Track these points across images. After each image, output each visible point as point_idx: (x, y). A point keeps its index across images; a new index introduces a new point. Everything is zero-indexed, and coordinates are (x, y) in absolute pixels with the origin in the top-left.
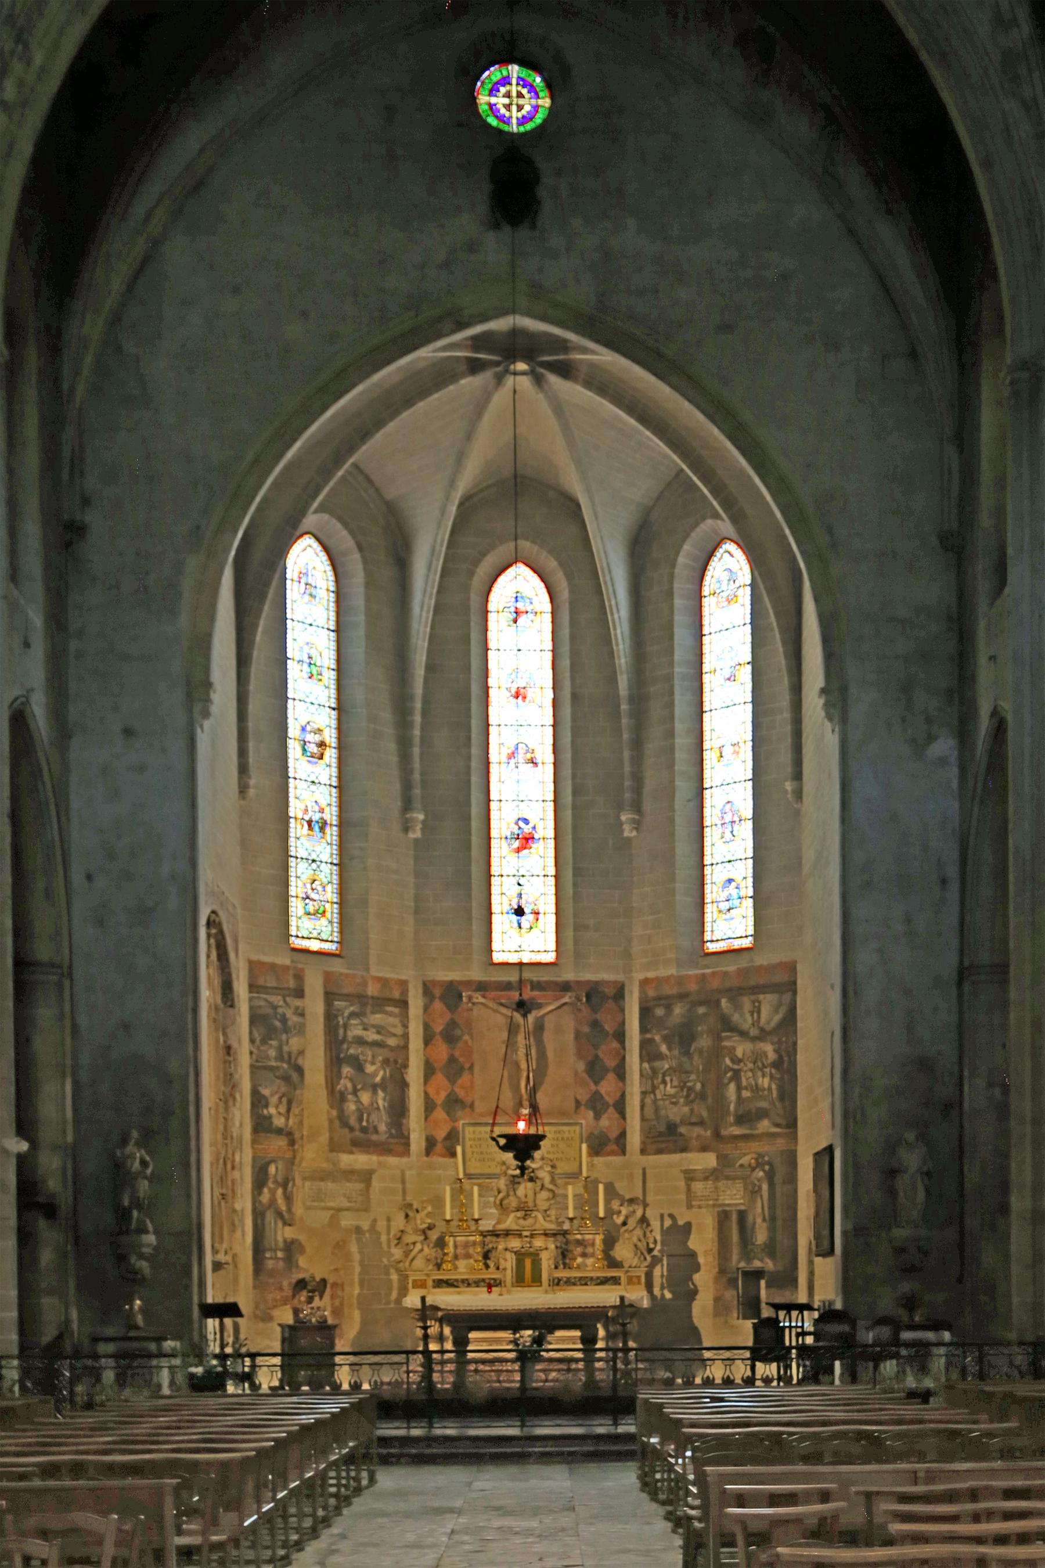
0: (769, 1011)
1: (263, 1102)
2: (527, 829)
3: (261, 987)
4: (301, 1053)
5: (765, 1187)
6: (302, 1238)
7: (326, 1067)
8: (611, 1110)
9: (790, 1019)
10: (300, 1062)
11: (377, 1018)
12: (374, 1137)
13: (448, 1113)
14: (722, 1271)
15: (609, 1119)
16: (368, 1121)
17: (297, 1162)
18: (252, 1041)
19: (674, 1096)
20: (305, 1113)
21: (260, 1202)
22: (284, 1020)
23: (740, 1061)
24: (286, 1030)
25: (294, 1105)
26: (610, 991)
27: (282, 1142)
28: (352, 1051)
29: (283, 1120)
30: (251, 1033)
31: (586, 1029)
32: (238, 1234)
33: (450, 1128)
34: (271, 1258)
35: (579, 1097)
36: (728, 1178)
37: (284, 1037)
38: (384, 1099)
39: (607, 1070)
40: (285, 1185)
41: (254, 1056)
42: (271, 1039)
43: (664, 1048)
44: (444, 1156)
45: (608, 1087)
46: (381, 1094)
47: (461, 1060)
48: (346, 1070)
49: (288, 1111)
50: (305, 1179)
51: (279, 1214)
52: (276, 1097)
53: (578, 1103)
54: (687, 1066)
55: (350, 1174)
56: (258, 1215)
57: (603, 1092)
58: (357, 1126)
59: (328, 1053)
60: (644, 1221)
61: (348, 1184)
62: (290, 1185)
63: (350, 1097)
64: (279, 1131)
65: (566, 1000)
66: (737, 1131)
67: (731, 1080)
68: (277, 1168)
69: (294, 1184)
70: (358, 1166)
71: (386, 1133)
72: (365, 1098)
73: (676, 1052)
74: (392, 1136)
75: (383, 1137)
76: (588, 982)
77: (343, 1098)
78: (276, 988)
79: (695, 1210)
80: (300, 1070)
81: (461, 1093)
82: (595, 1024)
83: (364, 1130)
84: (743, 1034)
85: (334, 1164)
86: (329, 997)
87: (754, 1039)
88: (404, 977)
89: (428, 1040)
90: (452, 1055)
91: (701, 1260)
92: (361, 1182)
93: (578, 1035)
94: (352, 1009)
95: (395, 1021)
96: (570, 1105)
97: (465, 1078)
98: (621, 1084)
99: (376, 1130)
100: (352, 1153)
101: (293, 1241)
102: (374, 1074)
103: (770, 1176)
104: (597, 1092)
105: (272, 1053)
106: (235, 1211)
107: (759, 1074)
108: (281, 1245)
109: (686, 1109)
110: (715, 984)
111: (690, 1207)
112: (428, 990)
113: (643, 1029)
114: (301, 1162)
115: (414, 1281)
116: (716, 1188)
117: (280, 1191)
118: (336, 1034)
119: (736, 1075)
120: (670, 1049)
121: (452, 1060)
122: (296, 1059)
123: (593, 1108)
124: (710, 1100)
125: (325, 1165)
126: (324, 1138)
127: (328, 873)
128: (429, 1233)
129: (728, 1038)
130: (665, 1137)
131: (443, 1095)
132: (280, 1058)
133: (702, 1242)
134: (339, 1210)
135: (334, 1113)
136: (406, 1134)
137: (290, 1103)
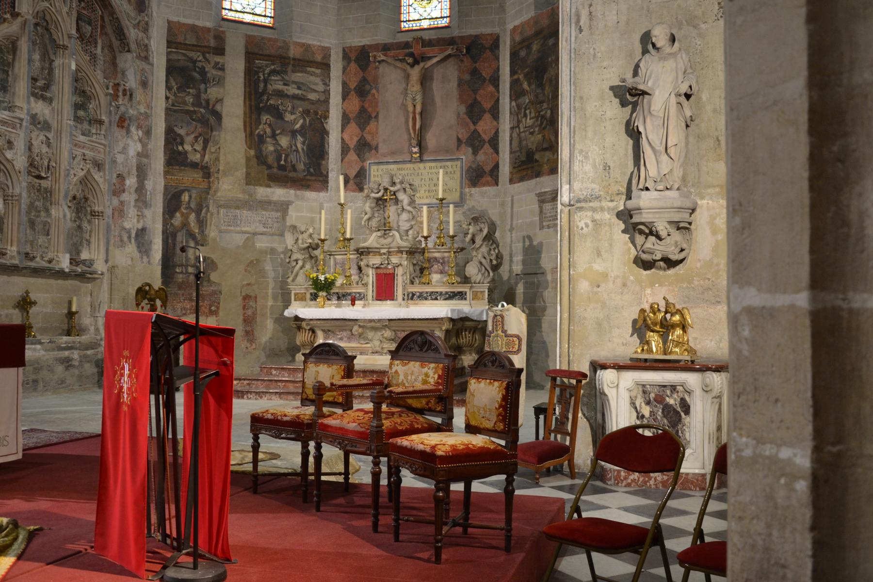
1: (179, 140)
3: (181, 43)
4: (220, 101)
7: (245, 113)
8: (487, 146)
10: (218, 108)
11: (298, 77)
12: (292, 174)
13: (358, 155)
15: (486, 154)
18: (168, 88)
19: (532, 127)
20: (222, 151)
21: (172, 224)
22: (203, 72)
24: (205, 80)
25: (211, 144)
27: (197, 175)
28: (272, 102)
29: (198, 156)
30: (167, 81)
31: (467, 77)
34: (182, 273)
35: (460, 137)
37: (202, 86)
38: (303, 143)
39: (485, 112)
40: (198, 212)
41: (170, 101)
42: (189, 88)
43: (525, 86)
44: (354, 191)
45: (485, 126)
46: (300, 139)
47: (369, 110)
48: (265, 117)
49: (204, 148)
50: (219, 206)
51: (192, 236)
52: (193, 136)
53: (459, 141)
55: (265, 204)
56: (169, 236)
57: (480, 131)
58: (276, 165)
59: (247, 102)
61: (264, 213)
62: (204, 211)
64: (194, 165)
65: (449, 52)
68: (190, 197)
69: (208, 210)
70: (275, 198)
71: (304, 171)
72: (284, 141)
73: (533, 87)
75: (301, 175)
76: (471, 36)
77: (261, 140)
78: (193, 45)
79: (546, 230)
80: (218, 116)
81: (368, 138)
82: (475, 72)
83: (282, 168)
85: (250, 195)
86: (251, 56)
88: (326, 45)
90: (363, 107)
92: (277, 211)
93: (460, 83)
94: (273, 67)
95: (318, 80)
96: (453, 143)
97: (372, 125)
98: (495, 123)
100: (270, 187)
102: (295, 122)
104: (475, 130)
105: (190, 99)
111: (542, 227)
112: (346, 56)
113: (513, 72)
117: (193, 216)
120: (529, 85)
122: (214, 106)
125: (240, 196)
126: (241, 173)
131: (356, 139)
132: (197, 103)
134: (255, 234)
135: (252, 152)
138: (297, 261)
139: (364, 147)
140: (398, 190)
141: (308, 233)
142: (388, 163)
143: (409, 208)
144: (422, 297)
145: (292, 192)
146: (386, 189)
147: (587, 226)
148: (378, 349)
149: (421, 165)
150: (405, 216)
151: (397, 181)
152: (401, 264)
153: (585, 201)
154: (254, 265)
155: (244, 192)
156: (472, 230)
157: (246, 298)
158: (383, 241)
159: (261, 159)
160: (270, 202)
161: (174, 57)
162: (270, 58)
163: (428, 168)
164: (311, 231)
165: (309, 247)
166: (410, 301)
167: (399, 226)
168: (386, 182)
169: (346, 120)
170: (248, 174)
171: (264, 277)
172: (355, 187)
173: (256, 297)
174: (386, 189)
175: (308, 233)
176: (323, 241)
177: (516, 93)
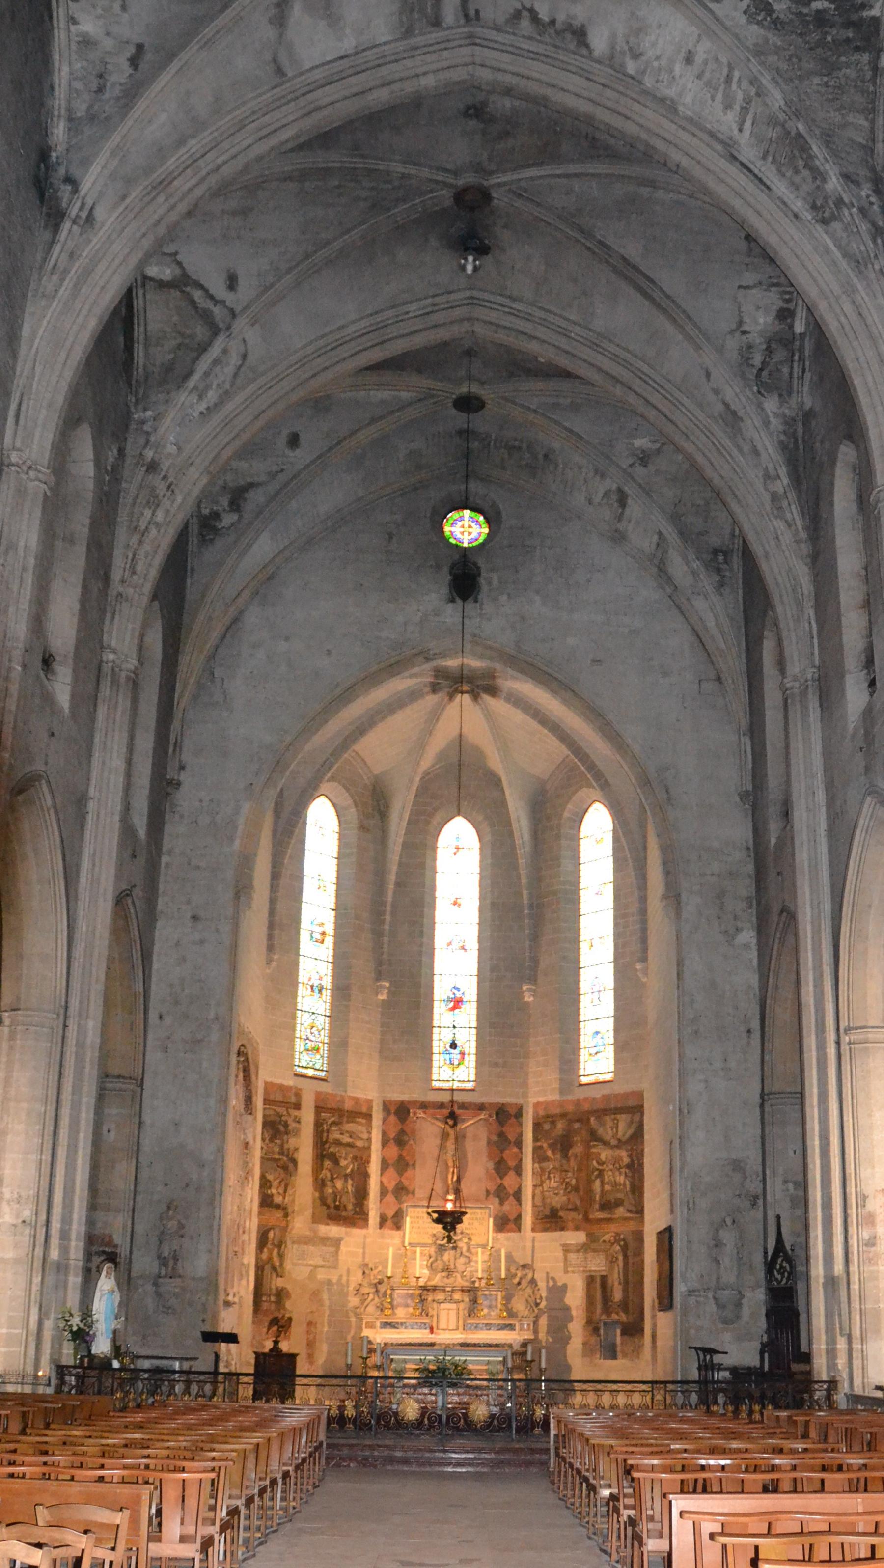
0: (623, 1127)
2: (458, 995)
4: (296, 1149)
5: (621, 1258)
6: (289, 1287)
8: (511, 1198)
9: (638, 1135)
10: (295, 1156)
12: (344, 1214)
14: (589, 1322)
18: (263, 1140)
19: (556, 1189)
22: (286, 1125)
23: (603, 1164)
26: (513, 1111)
27: (279, 1214)
28: (331, 1150)
29: (281, 1198)
31: (495, 1138)
32: (244, 1282)
36: (594, 1251)
37: (285, 1137)
39: (510, 1169)
43: (549, 1153)
44: (392, 1229)
45: (510, 1181)
46: (350, 1182)
48: (327, 1163)
49: (285, 1192)
50: (293, 1243)
51: (274, 1269)
53: (488, 1192)
54: (566, 1167)
55: (324, 1240)
56: (260, 1269)
58: (332, 1205)
60: (533, 1282)
63: (329, 1183)
64: (278, 1207)
66: (600, 1215)
67: (597, 1177)
72: (339, 1184)
73: (558, 1156)
74: (356, 1213)
75: (351, 1214)
80: (294, 1162)
81: (406, 1183)
82: (501, 1135)
83: (337, 1208)
84: (606, 1143)
86: (319, 1109)
87: (612, 1147)
89: (385, 1143)
93: (489, 1142)
97: (409, 1173)
101: (282, 1289)
102: (346, 1167)
103: (625, 1249)
105: (277, 1149)
106: (243, 1264)
107: (617, 1173)
108: (274, 1291)
109: (565, 1198)
110: (586, 1107)
111: (566, 1272)
113: (536, 1139)
117: (276, 1250)
118: (321, 1138)
119: (601, 1173)
120: (554, 1153)
121: (401, 1157)
123: (498, 1196)
124: (581, 1193)
125: (308, 1233)
126: (309, 1213)
127: (323, 1022)
128: (379, 1286)
129: (594, 1146)
130: (551, 1220)
131: (394, 1183)
132: (281, 1153)
133: (575, 1298)
134: (316, 1267)
135: (317, 1195)
137: (286, 1186)
139: (401, 1191)
150: (462, 1260)
154: (316, 1294)
156: (519, 1275)
157: (310, 1324)
158: (446, 1280)
159: (323, 1201)
161: (268, 1112)
162: (332, 1111)
164: (380, 1268)
169: (385, 1165)
170: (313, 1213)
177: (539, 1156)
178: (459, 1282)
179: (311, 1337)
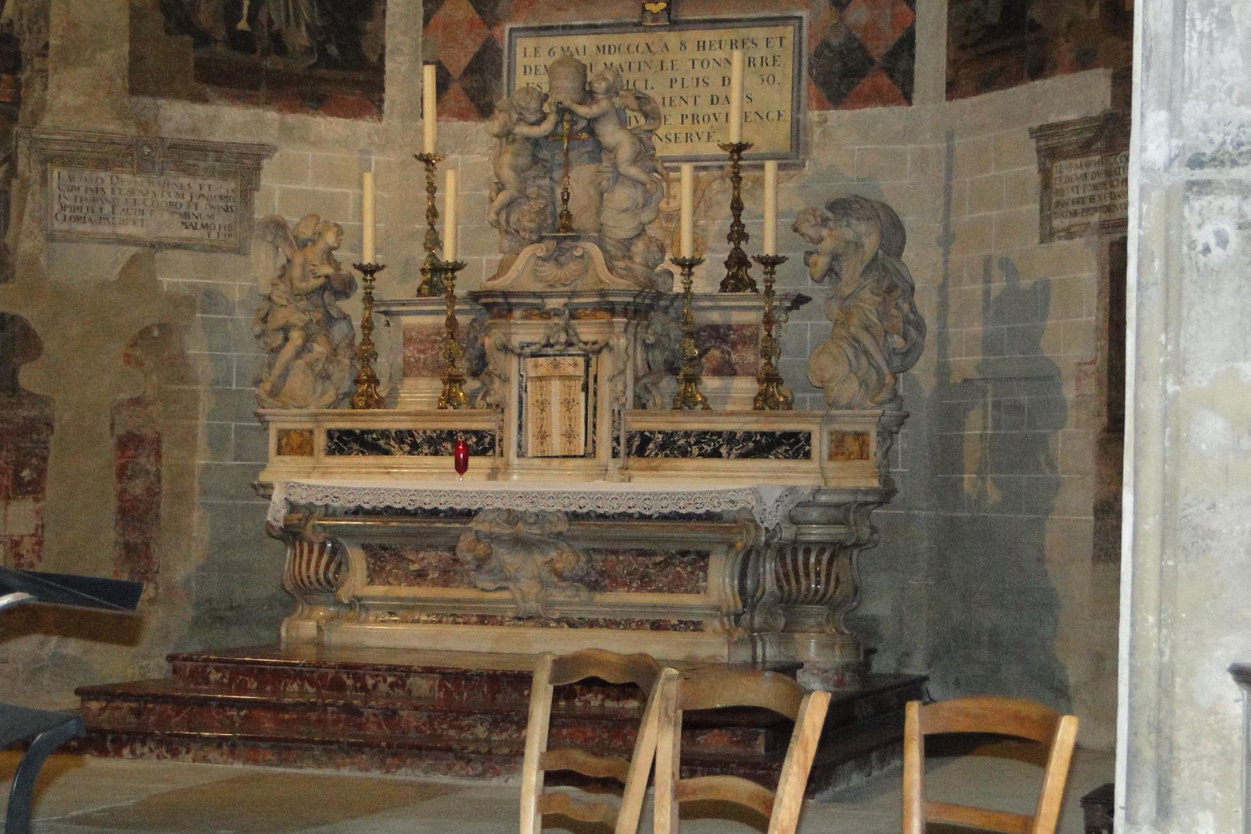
16: (252, 19)
17: (24, 114)
33: (480, 41)
44: (463, 116)
50: (48, 160)
55: (187, 154)
58: (221, 33)
61: (185, 180)
70: (219, 136)
71: (309, 51)
83: (241, 42)
85: (143, 126)
91: (1069, 393)
92: (225, 175)
99: (278, 45)
100: (204, 100)
111: (1047, 235)
114: (36, 117)
115: (284, 434)
116: (1108, 174)
125: (112, 127)
126: (114, 56)
134: (157, 246)
136: (374, 59)
138: (285, 330)
140: (604, 115)
141: (321, 246)
142: (568, 29)
143: (634, 171)
144: (673, 446)
145: (271, 115)
146: (562, 111)
147: (1223, 241)
148: (533, 606)
149: (673, 38)
150: (622, 196)
151: (600, 87)
152: (607, 345)
153: (1217, 161)
154: (156, 343)
155: (122, 115)
157: (129, 443)
160: (201, 149)
163: (692, 46)
164: (330, 238)
165: (323, 289)
166: (634, 462)
167: (600, 229)
168: (566, 91)
170: (136, 59)
171: (182, 379)
172: (465, 103)
173: (159, 441)
174: (562, 111)
175: (321, 246)
176: (369, 271)
178: (594, 268)
179: (138, 488)
